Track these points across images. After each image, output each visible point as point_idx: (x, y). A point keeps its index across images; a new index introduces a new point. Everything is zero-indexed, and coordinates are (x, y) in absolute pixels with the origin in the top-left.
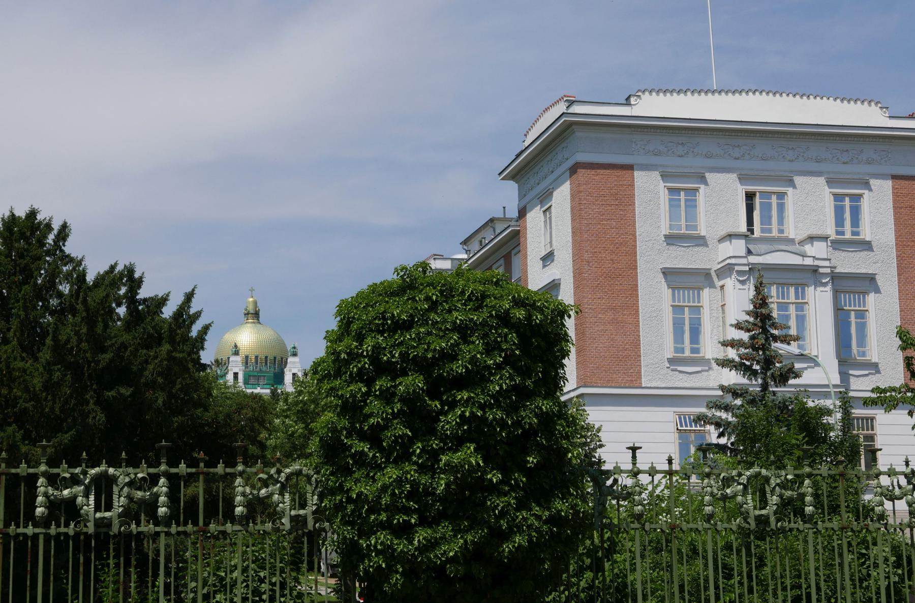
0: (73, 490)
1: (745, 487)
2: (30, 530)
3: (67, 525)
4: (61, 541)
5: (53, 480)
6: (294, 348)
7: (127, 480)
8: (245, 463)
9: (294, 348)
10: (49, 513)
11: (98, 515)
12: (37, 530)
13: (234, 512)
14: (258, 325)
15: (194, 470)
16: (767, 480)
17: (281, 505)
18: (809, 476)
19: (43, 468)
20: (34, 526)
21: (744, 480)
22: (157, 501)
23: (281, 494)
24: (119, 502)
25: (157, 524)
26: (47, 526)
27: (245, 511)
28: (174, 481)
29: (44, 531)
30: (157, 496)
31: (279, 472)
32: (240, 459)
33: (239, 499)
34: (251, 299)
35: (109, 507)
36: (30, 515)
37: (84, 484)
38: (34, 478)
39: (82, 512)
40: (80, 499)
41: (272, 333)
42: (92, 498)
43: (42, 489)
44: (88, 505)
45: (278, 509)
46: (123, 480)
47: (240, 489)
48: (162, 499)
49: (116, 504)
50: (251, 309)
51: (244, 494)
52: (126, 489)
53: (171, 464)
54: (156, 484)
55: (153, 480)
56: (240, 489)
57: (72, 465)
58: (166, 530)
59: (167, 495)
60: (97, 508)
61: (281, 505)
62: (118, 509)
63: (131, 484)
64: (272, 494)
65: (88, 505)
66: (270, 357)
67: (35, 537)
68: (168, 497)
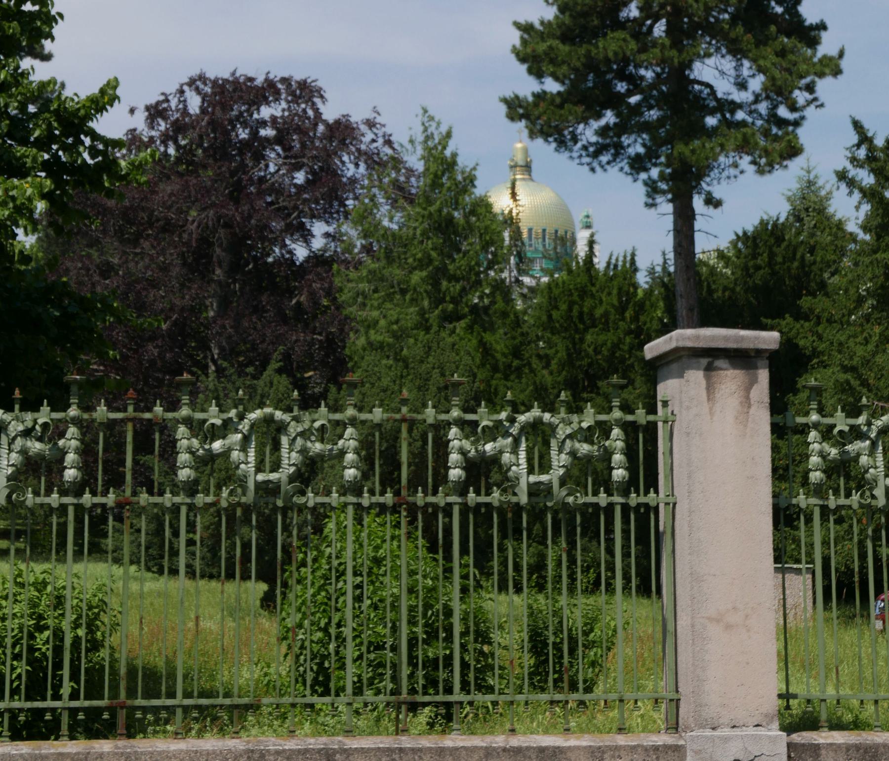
0: (497, 444)
1: (874, 444)
2: (603, 499)
3: (848, 495)
4: (483, 513)
5: (469, 428)
6: (588, 217)
7: (21, 428)
8: (193, 405)
9: (588, 217)
10: (467, 477)
11: (260, 477)
12: (67, 500)
13: (62, 476)
14: (531, 183)
15: (119, 415)
16: (553, 428)
17: (871, 470)
18: (353, 422)
19: (455, 413)
20: (609, 494)
21: (245, 426)
22: (62, 460)
23: (244, 449)
24: (559, 461)
25: (63, 493)
26: (79, 494)
27: (359, 475)
28: (86, 428)
29: (75, 501)
30: (63, 453)
31: (241, 417)
32: (185, 399)
33: (814, 460)
34: (519, 145)
35: (545, 467)
36: (441, 477)
37: (870, 439)
38: (441, 428)
39: (510, 474)
40: (235, 455)
41: (552, 194)
42: (252, 453)
43: (455, 443)
44: (518, 463)
45: (868, 476)
46: (15, 427)
47: (185, 442)
48: (71, 457)
49: (555, 463)
50: (520, 159)
51: (463, 452)
52: (299, 441)
53: (87, 407)
54: (62, 435)
55: (604, 429)
56: (185, 442)
57: (494, 408)
58: (188, 501)
59: (77, 451)
60: (259, 469)
61: (871, 470)
62: (287, 470)
63: (27, 433)
64: (501, 452)
65: (247, 463)
66: (550, 230)
67: (63, 508)
68: (625, 454)
